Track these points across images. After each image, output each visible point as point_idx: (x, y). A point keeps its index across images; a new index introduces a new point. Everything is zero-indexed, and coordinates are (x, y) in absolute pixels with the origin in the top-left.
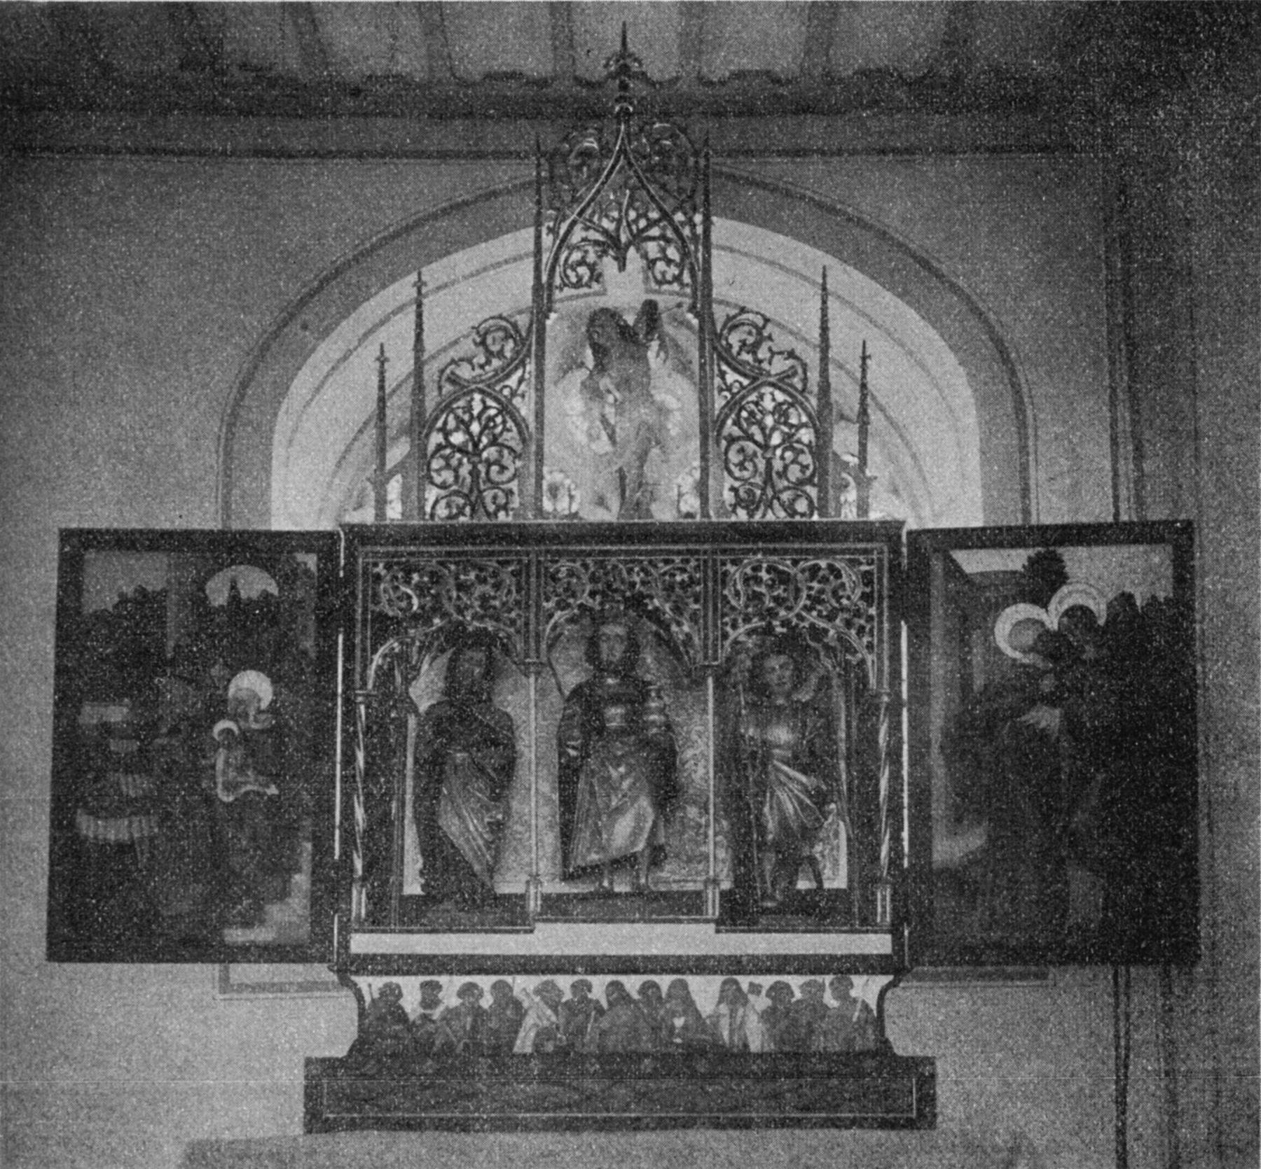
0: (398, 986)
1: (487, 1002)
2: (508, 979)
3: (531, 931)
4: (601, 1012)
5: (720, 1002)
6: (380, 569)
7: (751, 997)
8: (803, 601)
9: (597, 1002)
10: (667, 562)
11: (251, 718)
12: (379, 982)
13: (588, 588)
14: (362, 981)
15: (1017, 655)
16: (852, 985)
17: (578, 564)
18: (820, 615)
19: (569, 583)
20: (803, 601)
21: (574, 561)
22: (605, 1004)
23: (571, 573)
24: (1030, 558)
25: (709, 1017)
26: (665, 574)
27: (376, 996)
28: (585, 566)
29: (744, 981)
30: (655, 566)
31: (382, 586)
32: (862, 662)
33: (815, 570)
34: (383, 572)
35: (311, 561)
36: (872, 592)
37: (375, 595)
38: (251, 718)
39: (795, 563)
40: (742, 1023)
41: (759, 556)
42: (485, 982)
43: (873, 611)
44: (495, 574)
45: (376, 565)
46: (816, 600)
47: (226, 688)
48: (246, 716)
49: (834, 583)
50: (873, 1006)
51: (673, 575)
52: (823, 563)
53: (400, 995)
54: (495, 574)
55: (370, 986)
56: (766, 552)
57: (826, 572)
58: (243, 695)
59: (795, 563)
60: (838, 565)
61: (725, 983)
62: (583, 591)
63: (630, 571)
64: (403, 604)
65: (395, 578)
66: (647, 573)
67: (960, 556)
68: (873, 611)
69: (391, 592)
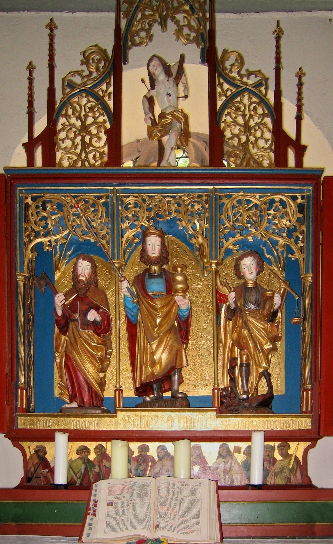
1: (92, 457)
2: (104, 444)
3: (115, 416)
5: (218, 458)
6: (29, 201)
7: (236, 455)
14: (25, 444)
16: (289, 447)
22: (156, 458)
23: (136, 205)
26: (188, 205)
27: (33, 452)
29: (232, 445)
31: (30, 211)
42: (92, 446)
45: (26, 198)
50: (301, 459)
51: (193, 206)
53: (45, 453)
55: (29, 447)
61: (221, 447)
64: (43, 223)
68: (304, 228)
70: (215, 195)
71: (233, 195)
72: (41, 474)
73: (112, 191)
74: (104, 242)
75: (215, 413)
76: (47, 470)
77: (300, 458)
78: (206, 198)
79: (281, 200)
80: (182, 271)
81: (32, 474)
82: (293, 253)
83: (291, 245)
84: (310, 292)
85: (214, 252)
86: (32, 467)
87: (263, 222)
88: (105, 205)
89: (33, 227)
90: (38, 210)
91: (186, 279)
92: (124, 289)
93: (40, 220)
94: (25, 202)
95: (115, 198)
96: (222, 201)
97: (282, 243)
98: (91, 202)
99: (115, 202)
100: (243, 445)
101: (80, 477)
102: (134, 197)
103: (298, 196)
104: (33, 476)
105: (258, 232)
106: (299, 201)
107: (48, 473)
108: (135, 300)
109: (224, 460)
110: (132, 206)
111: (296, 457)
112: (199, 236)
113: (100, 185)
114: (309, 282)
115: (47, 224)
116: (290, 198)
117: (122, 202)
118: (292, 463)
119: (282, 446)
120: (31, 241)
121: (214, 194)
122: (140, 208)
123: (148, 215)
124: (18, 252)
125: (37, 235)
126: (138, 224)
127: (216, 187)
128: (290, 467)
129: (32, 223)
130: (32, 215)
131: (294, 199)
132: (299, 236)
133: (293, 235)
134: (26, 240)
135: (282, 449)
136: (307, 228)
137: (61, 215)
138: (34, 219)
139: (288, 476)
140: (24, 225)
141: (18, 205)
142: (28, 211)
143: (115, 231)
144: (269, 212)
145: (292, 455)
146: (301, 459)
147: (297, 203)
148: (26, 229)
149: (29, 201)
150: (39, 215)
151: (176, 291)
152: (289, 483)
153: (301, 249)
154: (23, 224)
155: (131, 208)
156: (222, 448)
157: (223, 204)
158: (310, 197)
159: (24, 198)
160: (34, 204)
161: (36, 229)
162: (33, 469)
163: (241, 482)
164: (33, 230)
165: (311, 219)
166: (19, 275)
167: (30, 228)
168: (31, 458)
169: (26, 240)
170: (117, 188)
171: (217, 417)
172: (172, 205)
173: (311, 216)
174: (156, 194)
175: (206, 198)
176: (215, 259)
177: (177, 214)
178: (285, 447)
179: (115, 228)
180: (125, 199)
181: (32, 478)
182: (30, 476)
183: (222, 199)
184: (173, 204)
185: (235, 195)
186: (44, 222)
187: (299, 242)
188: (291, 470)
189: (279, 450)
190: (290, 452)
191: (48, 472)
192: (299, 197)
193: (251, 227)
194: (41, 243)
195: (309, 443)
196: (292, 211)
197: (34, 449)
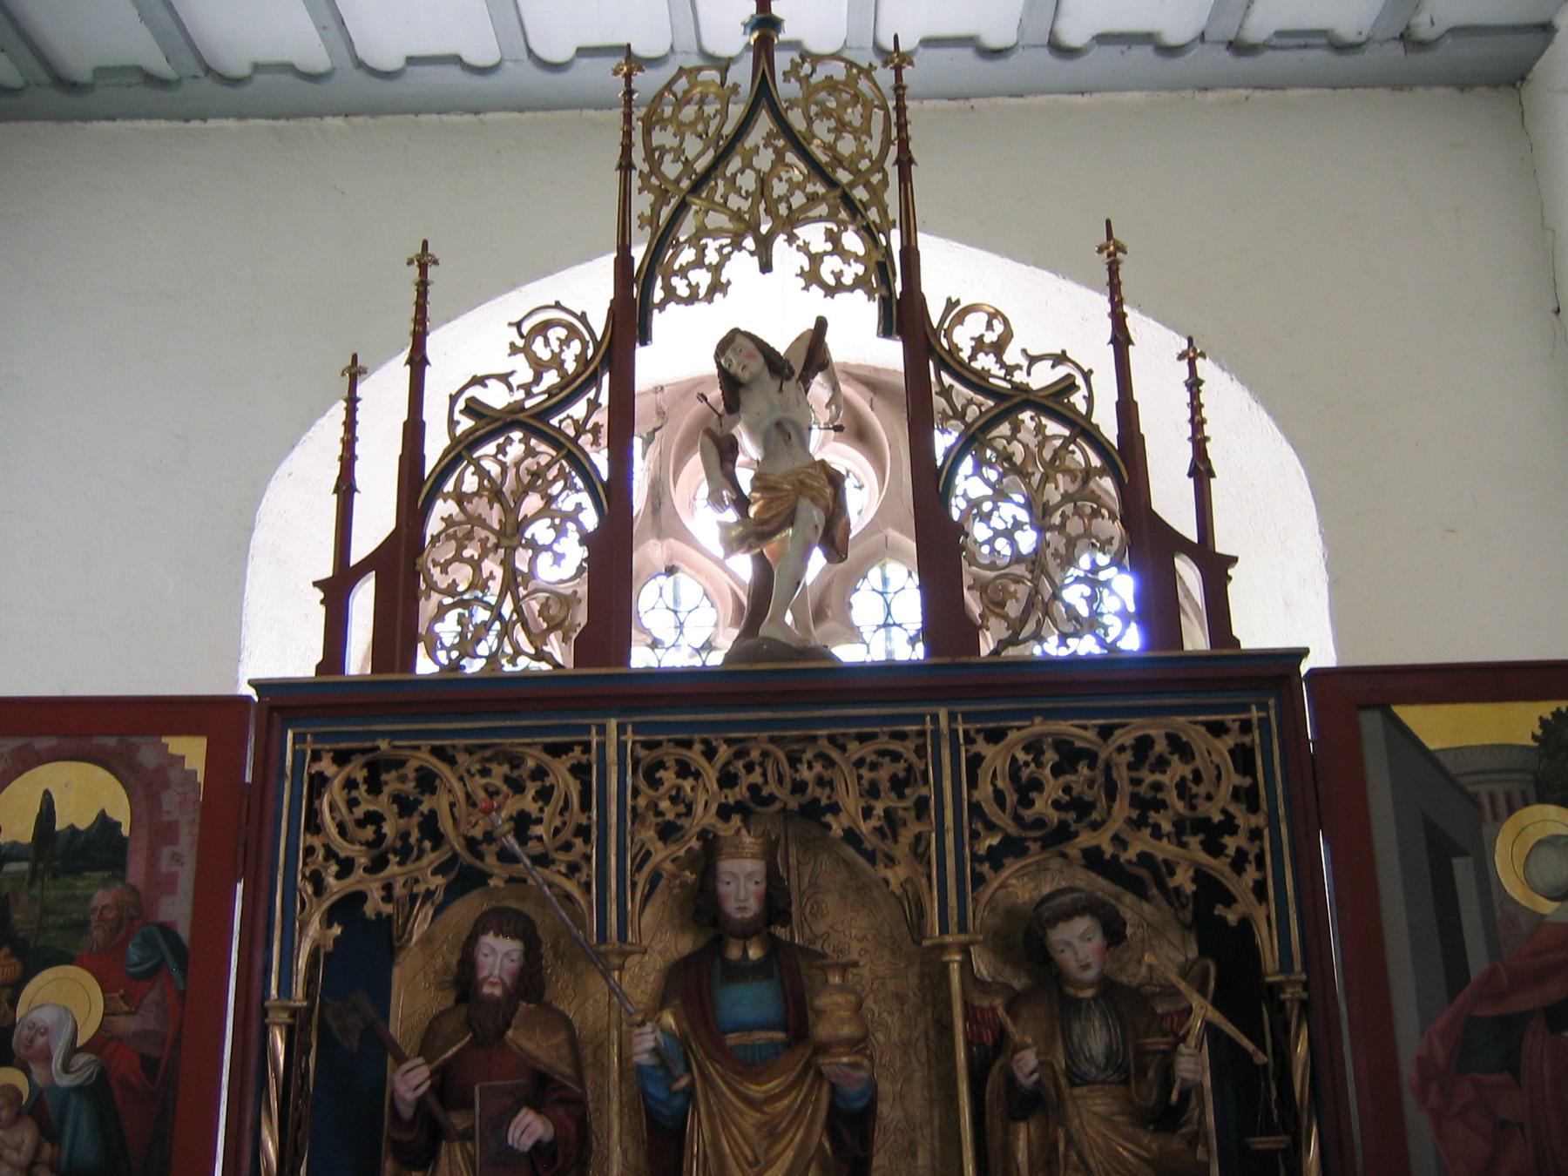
6: (326, 766)
10: (863, 738)
11: (57, 1063)
15: (1547, 907)
18: (1157, 833)
19: (679, 789)
20: (1122, 810)
24: (1543, 723)
26: (859, 763)
28: (710, 753)
32: (1246, 924)
33: (1143, 745)
35: (192, 751)
36: (1255, 786)
37: (313, 813)
38: (57, 1063)
39: (1105, 732)
44: (539, 773)
46: (1146, 805)
47: (13, 1003)
48: (46, 1057)
49: (1179, 769)
54: (539, 773)
56: (1048, 714)
58: (46, 1016)
59: (1105, 732)
63: (794, 761)
64: (369, 833)
66: (829, 762)
67: (1412, 716)
69: (344, 810)
71: (1011, 728)
74: (570, 886)
78: (920, 741)
82: (1229, 900)
90: (354, 793)
93: (361, 824)
98: (531, 763)
103: (1230, 724)
115: (380, 837)
116: (1202, 729)
123: (723, 800)
130: (331, 809)
133: (1225, 847)
140: (304, 840)
142: (320, 795)
144: (1135, 774)
149: (326, 766)
150: (354, 810)
164: (330, 854)
167: (321, 853)
172: (804, 768)
175: (920, 741)
185: (1019, 728)
186: (370, 829)
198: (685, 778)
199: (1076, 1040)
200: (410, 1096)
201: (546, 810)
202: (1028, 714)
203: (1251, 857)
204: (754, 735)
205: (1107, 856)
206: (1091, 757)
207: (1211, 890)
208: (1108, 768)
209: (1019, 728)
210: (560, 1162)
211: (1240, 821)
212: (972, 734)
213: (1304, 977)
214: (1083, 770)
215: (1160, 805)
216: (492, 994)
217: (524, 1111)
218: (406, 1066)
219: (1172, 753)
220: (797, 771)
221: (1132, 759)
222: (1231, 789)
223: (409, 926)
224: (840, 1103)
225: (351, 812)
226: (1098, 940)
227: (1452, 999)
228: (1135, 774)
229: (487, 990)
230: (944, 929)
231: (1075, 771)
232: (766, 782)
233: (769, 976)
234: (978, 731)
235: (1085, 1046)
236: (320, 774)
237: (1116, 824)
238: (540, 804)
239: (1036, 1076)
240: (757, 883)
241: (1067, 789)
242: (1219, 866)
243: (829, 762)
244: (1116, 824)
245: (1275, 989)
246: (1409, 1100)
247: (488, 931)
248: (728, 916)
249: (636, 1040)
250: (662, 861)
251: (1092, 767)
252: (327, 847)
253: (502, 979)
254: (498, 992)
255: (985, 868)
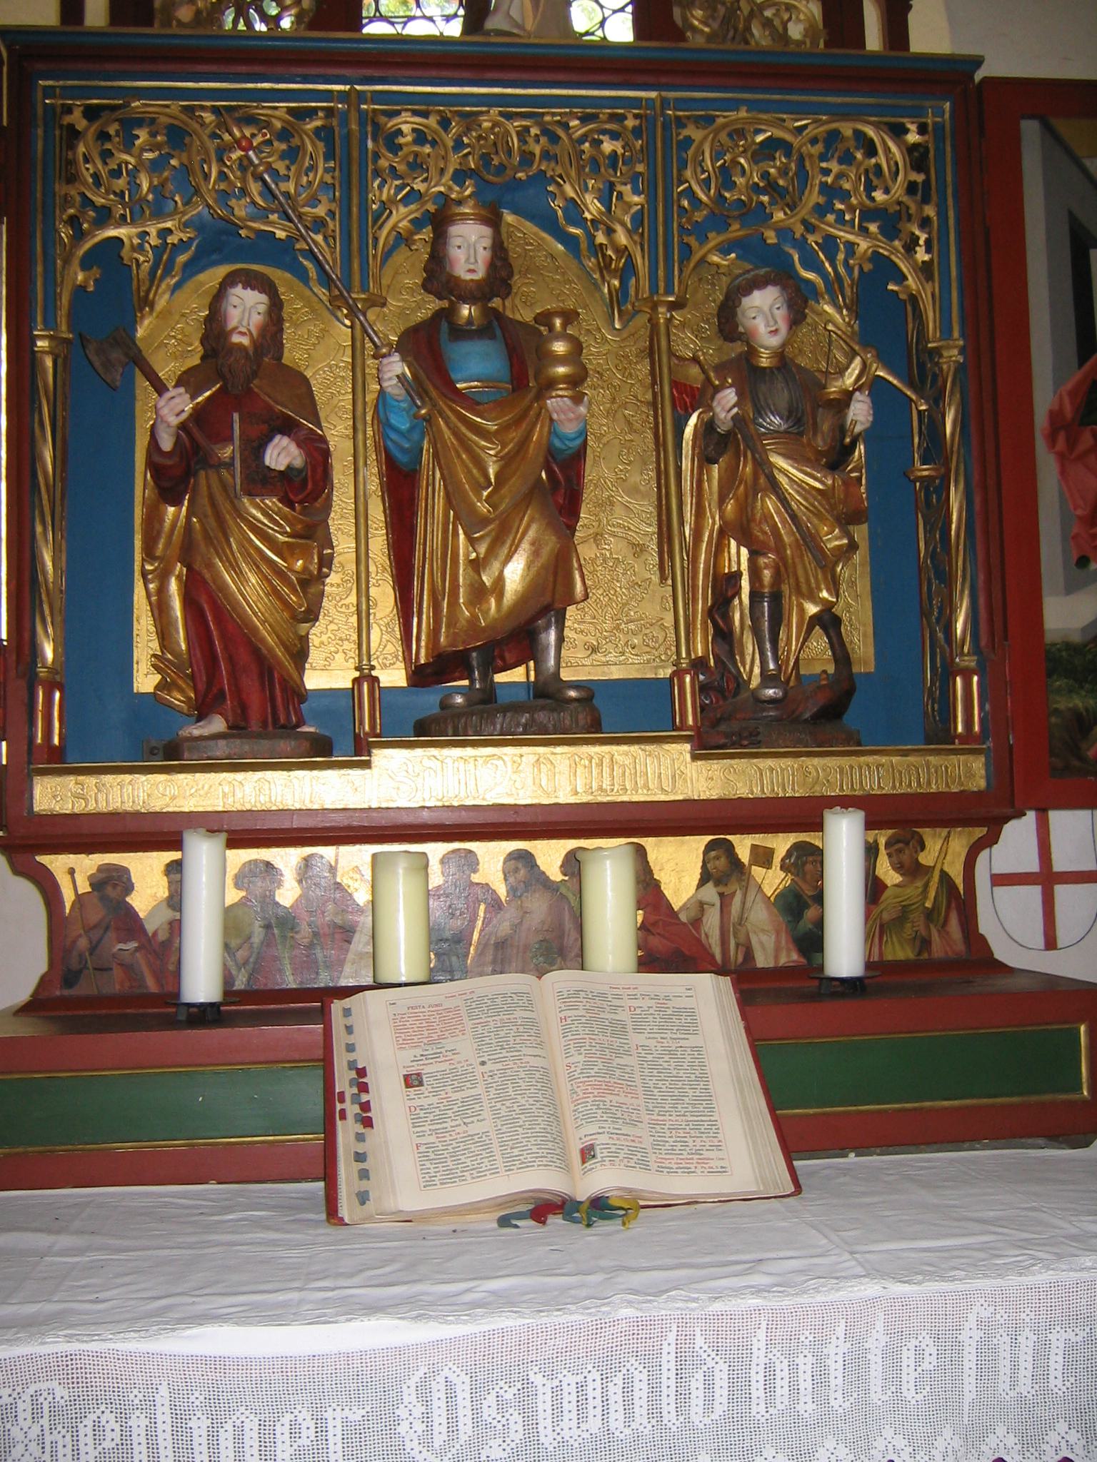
0: (125, 871)
3: (367, 765)
4: (495, 905)
5: (703, 881)
7: (757, 872)
8: (814, 197)
9: (486, 887)
12: (88, 864)
13: (454, 162)
14: (57, 863)
17: (432, 121)
20: (814, 197)
21: (425, 114)
22: (502, 891)
23: (420, 137)
25: (684, 907)
27: (84, 887)
29: (743, 845)
30: (566, 126)
31: (81, 149)
34: (81, 124)
40: (741, 920)
41: (743, 113)
42: (287, 859)
43: (930, 211)
45: (69, 110)
50: (959, 882)
52: (847, 129)
53: (129, 888)
54: (284, 135)
55: (72, 872)
56: (752, 105)
57: (852, 144)
60: (870, 132)
61: (710, 847)
62: (442, 171)
65: (103, 136)
66: (554, 139)
68: (930, 211)
70: (663, 114)
71: (718, 116)
72: (114, 956)
73: (343, 96)
75: (688, 747)
76: (132, 945)
77: (956, 872)
78: (637, 122)
79: (859, 135)
80: (564, 325)
81: (80, 963)
83: (893, 257)
84: (957, 389)
85: (661, 273)
86: (80, 936)
87: (807, 192)
88: (325, 134)
89: (89, 195)
90: (108, 146)
91: (577, 347)
92: (390, 379)
94: (65, 123)
95: (354, 116)
96: (685, 132)
97: (866, 251)
98: (278, 125)
99: (354, 127)
100: (782, 844)
101: (245, 963)
102: (415, 113)
103: (909, 126)
104: (85, 967)
105: (792, 220)
106: (913, 137)
107: (138, 954)
108: (423, 412)
109: (721, 889)
110: (409, 138)
111: (945, 876)
112: (619, 228)
113: (305, 80)
114: (954, 362)
116: (885, 128)
117: (376, 125)
118: (932, 894)
119: (898, 841)
120: (80, 235)
121: (658, 111)
122: (434, 143)
124: (40, 269)
125: (104, 217)
126: (428, 190)
127: (664, 94)
128: (928, 904)
129: (85, 183)
131: (898, 131)
132: (917, 232)
134: (65, 233)
135: (900, 851)
136: (938, 214)
137: (179, 159)
138: (91, 171)
139: (924, 933)
140: (61, 188)
141: (40, 132)
143: (355, 210)
144: (824, 165)
145: (929, 870)
146: (959, 882)
147: (905, 142)
148: (67, 202)
150: (108, 161)
151: (551, 384)
152: (925, 956)
153: (925, 270)
154: (57, 186)
155: (407, 144)
156: (713, 854)
157: (689, 140)
158: (944, 127)
159: (59, 110)
160: (92, 129)
161: (100, 201)
162: (83, 943)
163: (776, 957)
164: (87, 202)
165: (950, 191)
166: (42, 337)
167: (78, 199)
168: (78, 906)
169: (65, 233)
170: (358, 87)
171: (695, 758)
173: (949, 179)
174: (484, 109)
175: (637, 122)
176: (669, 291)
177: (548, 166)
178: (907, 844)
179: (355, 201)
180: (386, 119)
181: (80, 971)
182: (74, 965)
183: (684, 126)
184: (538, 141)
185: (725, 117)
187: (918, 249)
188: (929, 915)
189: (889, 855)
190: (926, 858)
191: (137, 949)
192: (913, 127)
193: (771, 203)
194: (118, 240)
195: (980, 832)
196: (892, 163)
197: (90, 878)
198: (422, 144)
199: (761, 397)
200: (174, 421)
201: (293, 168)
202: (734, 105)
203: (921, 242)
204: (484, 109)
205: (797, 236)
206: (787, 147)
207: (883, 268)
208: (801, 159)
209: (725, 117)
210: (310, 486)
211: (913, 210)
212: (685, 121)
213: (961, 343)
214: (781, 159)
215: (845, 196)
216: (240, 346)
217: (278, 438)
218: (168, 395)
219: (857, 148)
220: (526, 142)
221: (823, 150)
222: (905, 185)
223: (151, 296)
224: (557, 443)
225: (105, 163)
226: (781, 314)
227: (1081, 364)
228: (824, 165)
229: (236, 339)
230: (654, 288)
231: (774, 159)
232: (497, 153)
233: (493, 337)
234: (688, 117)
235: (770, 402)
236: (71, 127)
237: (804, 211)
238: (287, 162)
239: (735, 410)
240: (485, 248)
241: (764, 176)
242: (893, 250)
243: (554, 139)
244: (804, 211)
245: (937, 352)
246: (1040, 445)
247: (237, 284)
248: (457, 279)
249: (385, 369)
250: (400, 221)
251: (788, 155)
252: (83, 195)
253: (249, 330)
254: (245, 341)
255: (692, 241)
